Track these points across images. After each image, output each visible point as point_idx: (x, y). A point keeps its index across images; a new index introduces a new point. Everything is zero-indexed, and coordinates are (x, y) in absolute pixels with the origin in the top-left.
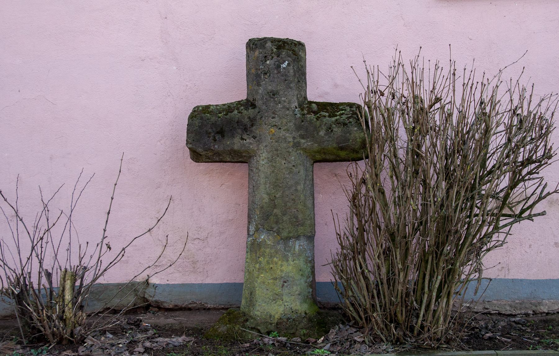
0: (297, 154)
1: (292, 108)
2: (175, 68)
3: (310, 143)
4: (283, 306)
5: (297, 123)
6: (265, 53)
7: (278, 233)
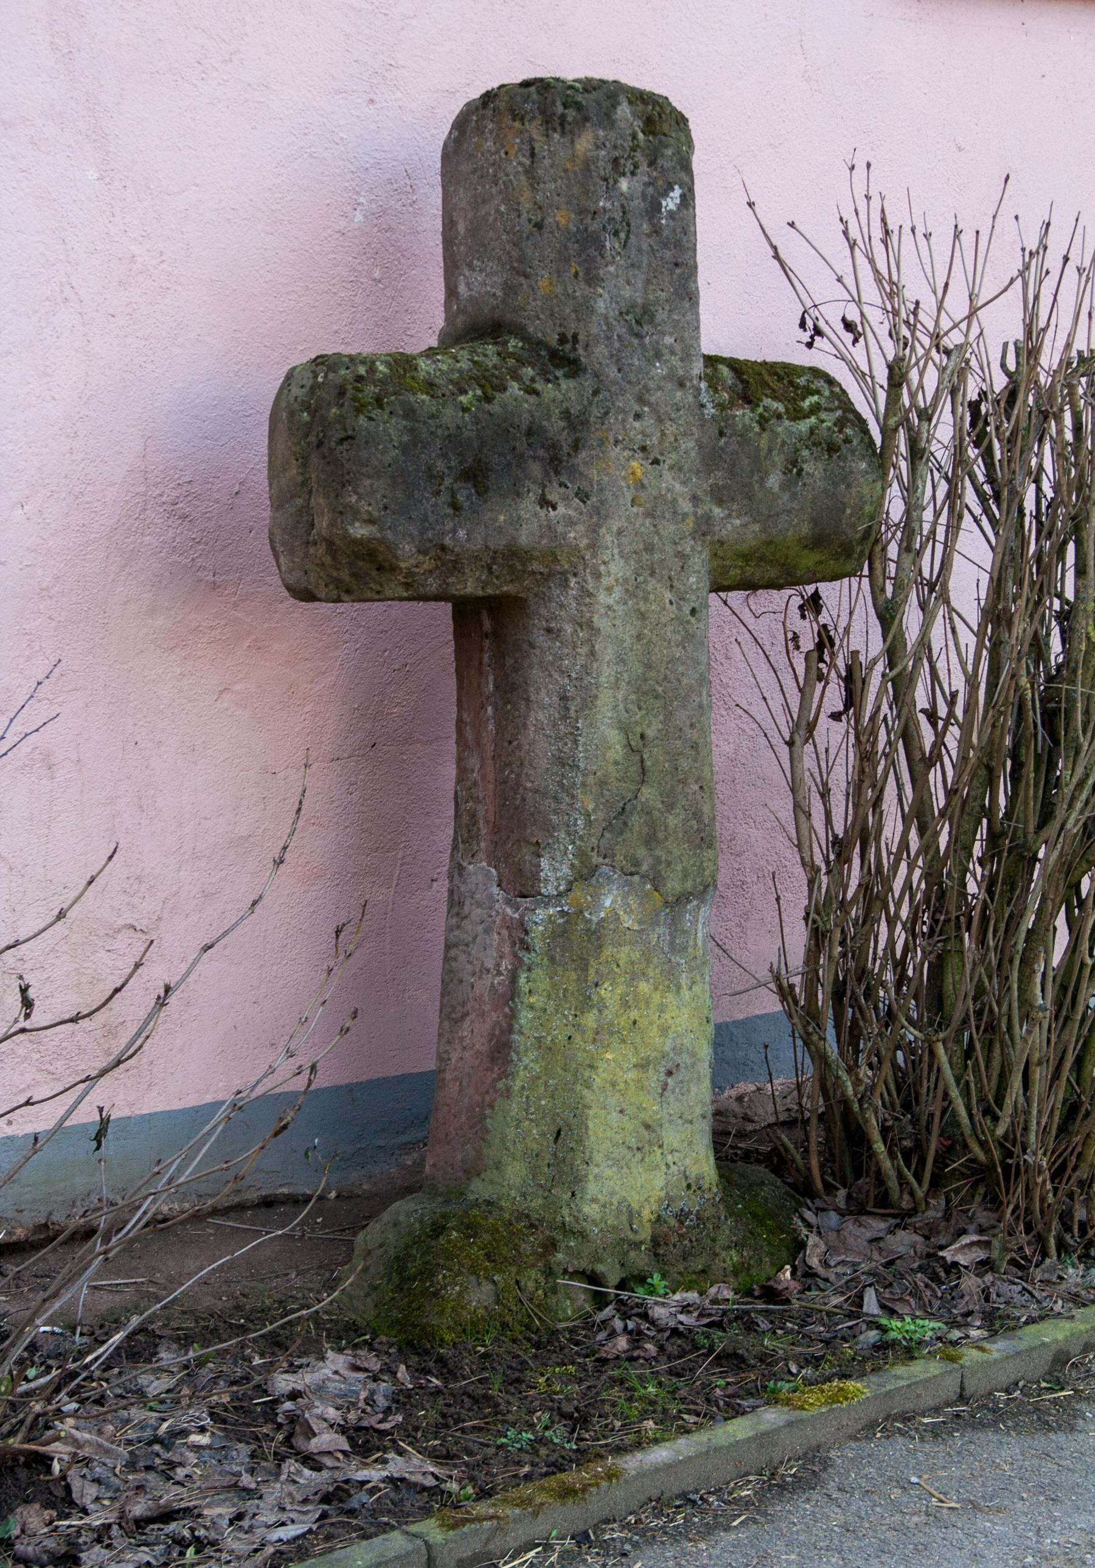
7: (657, 882)
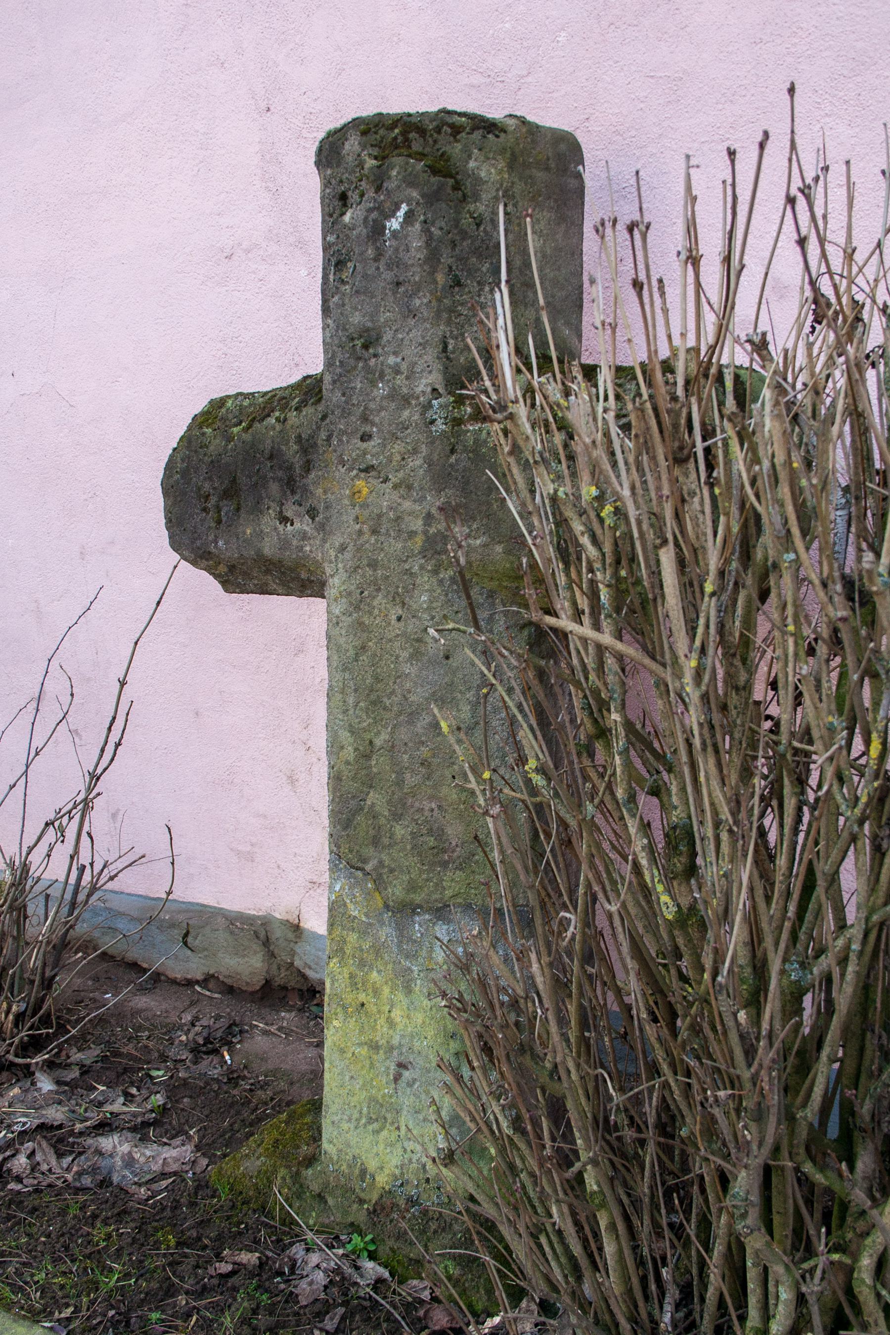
0: (441, 582)
1: (418, 398)
2: (304, 272)
3: (478, 542)
4: (400, 1151)
5: (435, 457)
6: (341, 181)
7: (380, 884)
